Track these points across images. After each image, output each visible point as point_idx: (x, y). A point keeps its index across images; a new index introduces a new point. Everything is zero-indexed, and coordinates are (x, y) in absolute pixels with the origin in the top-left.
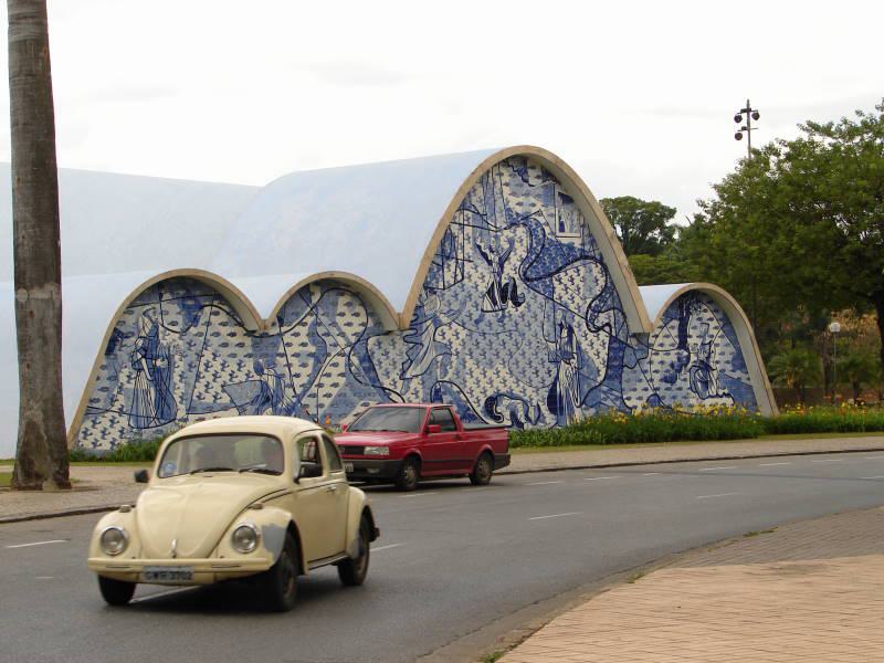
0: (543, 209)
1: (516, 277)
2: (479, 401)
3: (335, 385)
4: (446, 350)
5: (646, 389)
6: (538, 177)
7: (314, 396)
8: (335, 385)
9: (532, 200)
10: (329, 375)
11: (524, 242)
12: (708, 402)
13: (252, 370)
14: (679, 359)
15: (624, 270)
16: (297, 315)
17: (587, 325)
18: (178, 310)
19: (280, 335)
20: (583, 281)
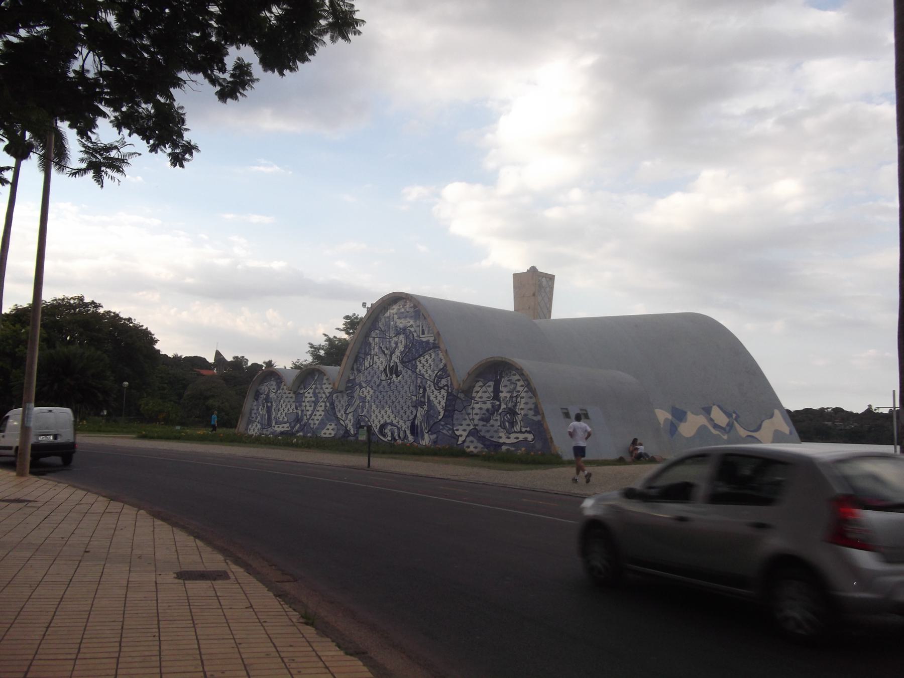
1: (398, 361)
2: (376, 426)
3: (320, 415)
4: (363, 399)
5: (469, 425)
7: (313, 419)
8: (320, 415)
10: (318, 411)
11: (403, 343)
12: (513, 436)
14: (493, 407)
16: (310, 384)
17: (434, 386)
20: (434, 360)
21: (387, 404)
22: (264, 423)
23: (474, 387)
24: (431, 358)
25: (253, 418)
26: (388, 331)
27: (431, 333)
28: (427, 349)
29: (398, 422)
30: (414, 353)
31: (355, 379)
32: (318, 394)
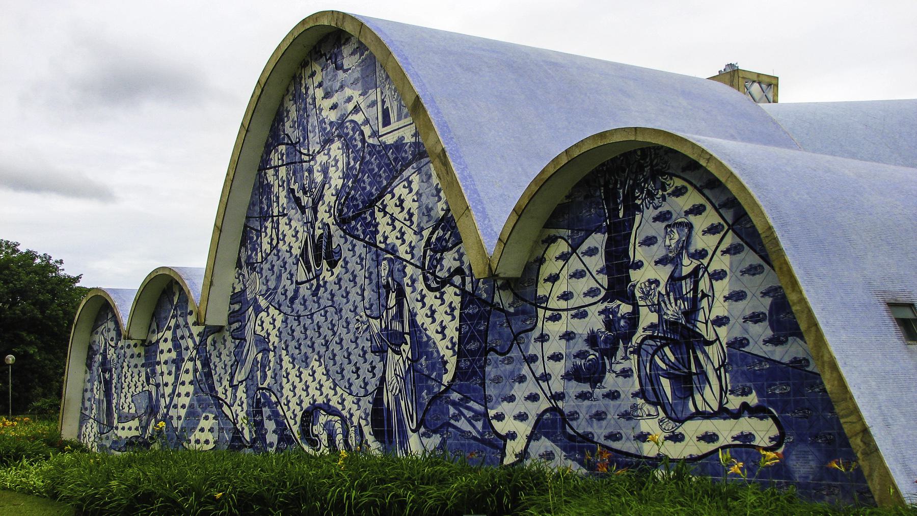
1: (330, 221)
2: (295, 416)
3: (187, 395)
5: (533, 398)
6: (353, 54)
7: (175, 406)
8: (187, 395)
10: (183, 383)
11: (340, 164)
14: (609, 324)
16: (167, 320)
17: (426, 279)
19: (158, 341)
21: (314, 350)
23: (541, 261)
24: (411, 191)
25: (86, 409)
26: (304, 140)
27: (406, 117)
28: (399, 167)
30: (368, 188)
31: (243, 291)
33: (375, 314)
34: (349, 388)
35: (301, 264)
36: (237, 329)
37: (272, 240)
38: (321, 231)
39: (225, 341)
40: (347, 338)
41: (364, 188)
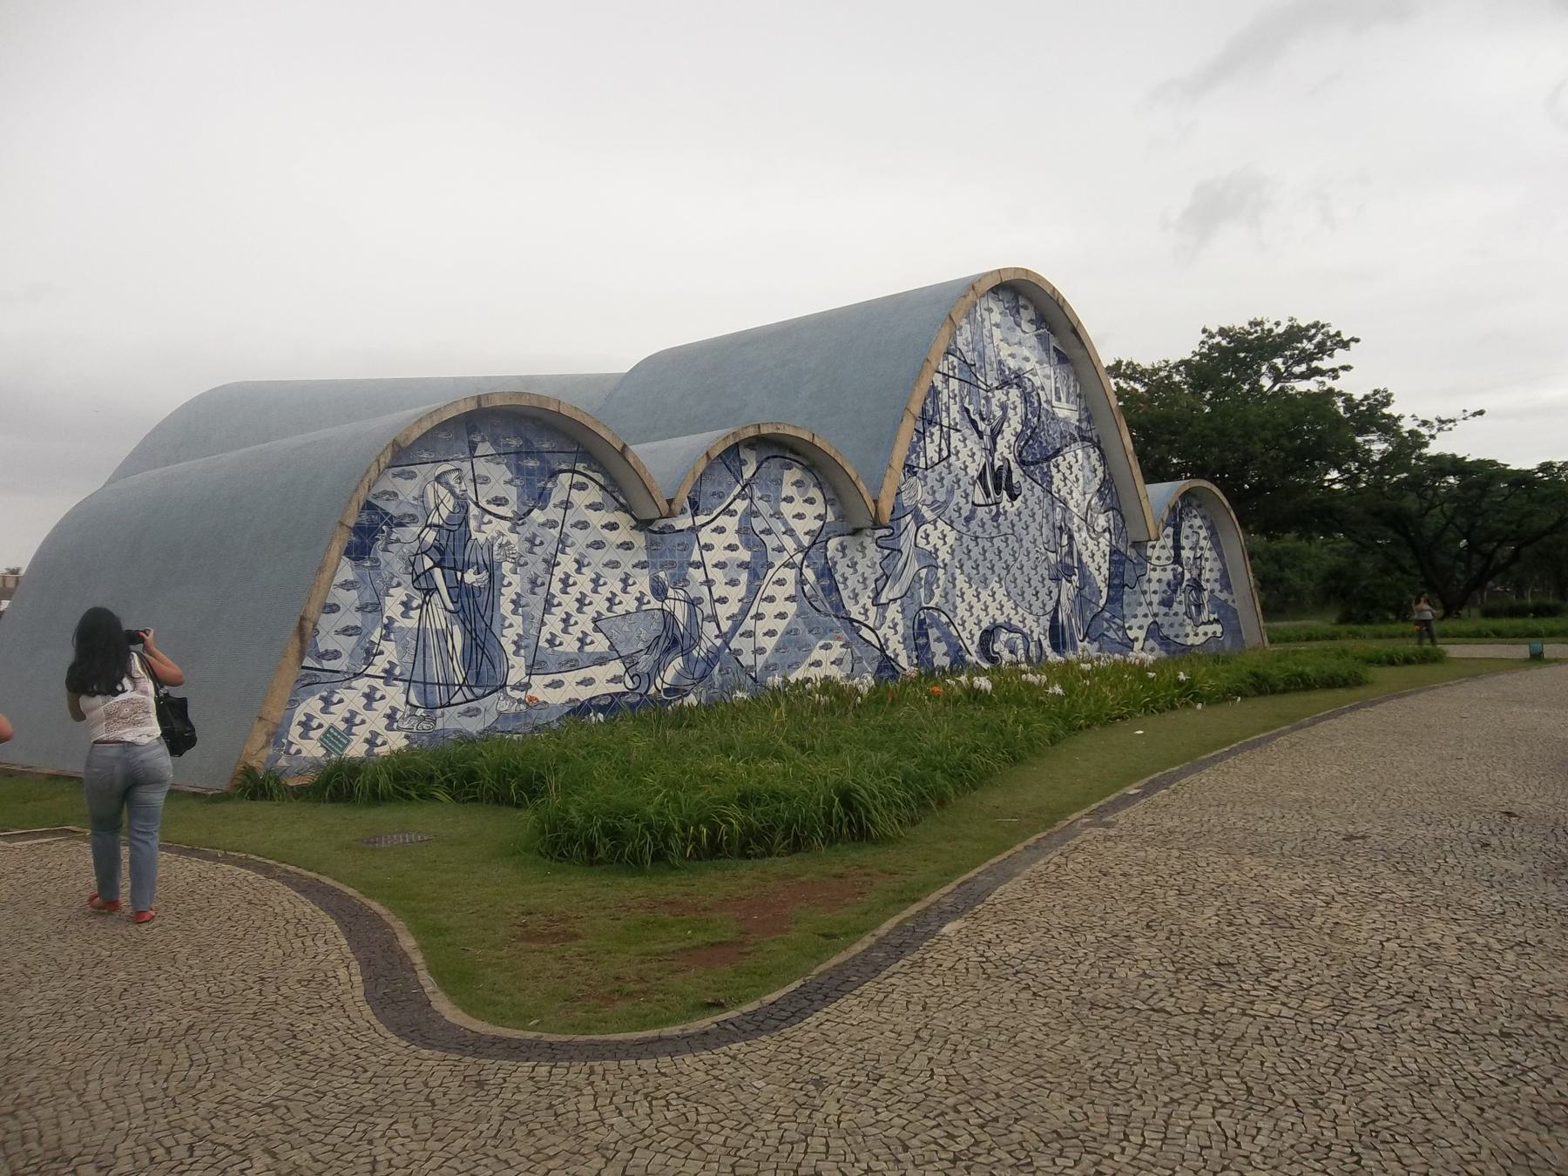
0: (1038, 366)
1: (1011, 457)
2: (972, 635)
3: (782, 616)
4: (930, 560)
5: (1146, 616)
6: (1031, 321)
7: (750, 634)
8: (782, 616)
9: (1027, 353)
10: (771, 599)
11: (1018, 410)
13: (647, 591)
14: (1175, 576)
15: (1130, 457)
16: (721, 496)
17: (1088, 529)
18: (509, 476)
19: (694, 529)
20: (1082, 468)
21: (994, 572)
22: (435, 671)
29: (1023, 622)
32: (762, 536)
33: (1053, 549)
34: (1030, 608)
35: (978, 488)
36: (886, 536)
37: (941, 450)
38: (1001, 463)
39: (864, 548)
40: (1028, 565)
41: (1041, 443)
